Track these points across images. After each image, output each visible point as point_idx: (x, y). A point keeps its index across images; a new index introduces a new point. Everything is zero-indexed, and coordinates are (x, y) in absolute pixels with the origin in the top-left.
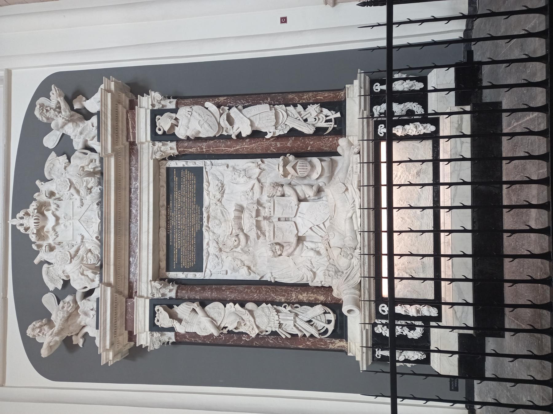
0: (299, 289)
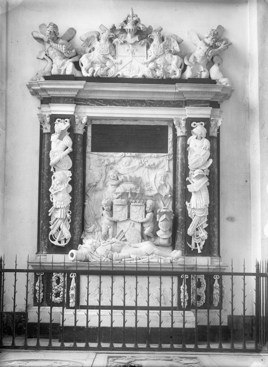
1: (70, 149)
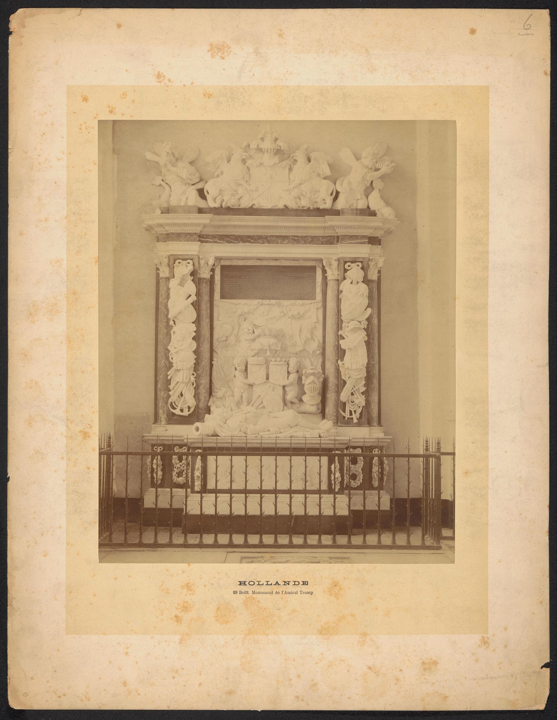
1: (194, 298)
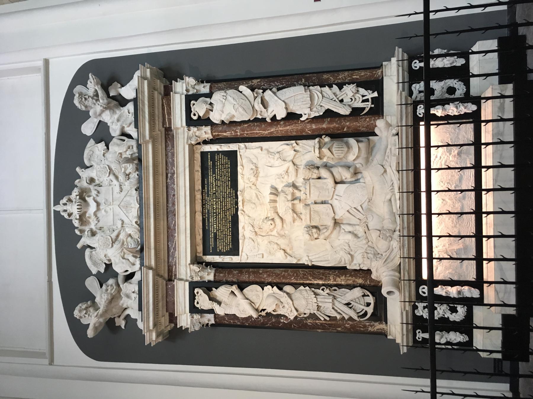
0: (337, 272)
1: (234, 288)
